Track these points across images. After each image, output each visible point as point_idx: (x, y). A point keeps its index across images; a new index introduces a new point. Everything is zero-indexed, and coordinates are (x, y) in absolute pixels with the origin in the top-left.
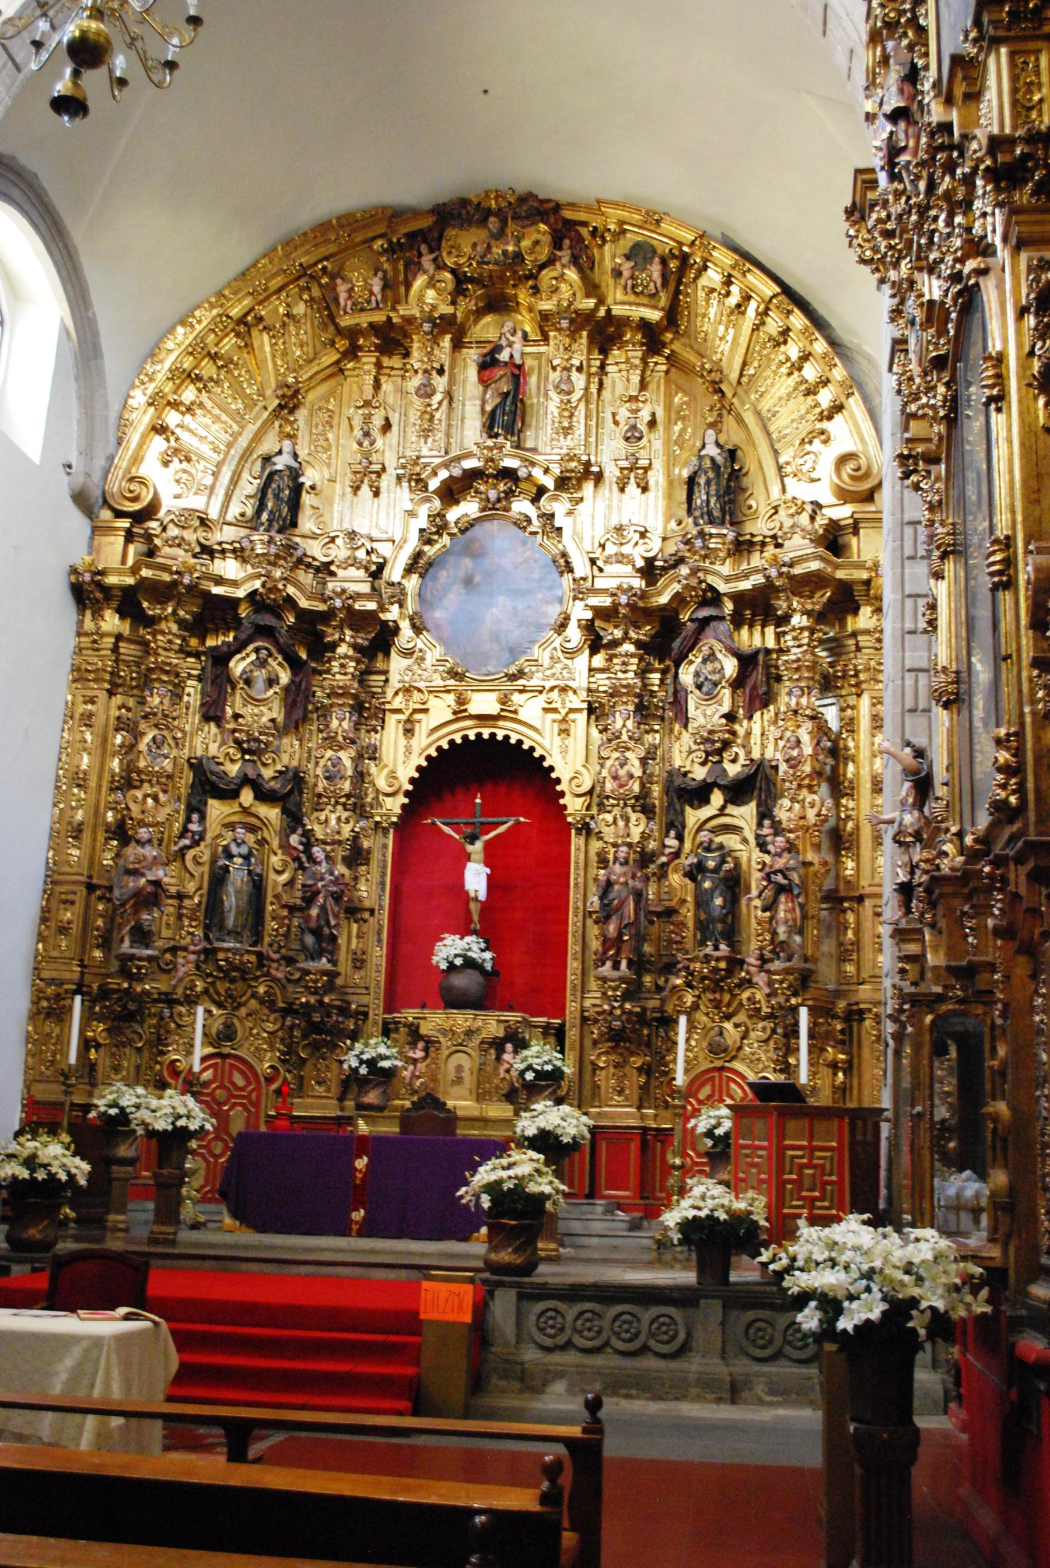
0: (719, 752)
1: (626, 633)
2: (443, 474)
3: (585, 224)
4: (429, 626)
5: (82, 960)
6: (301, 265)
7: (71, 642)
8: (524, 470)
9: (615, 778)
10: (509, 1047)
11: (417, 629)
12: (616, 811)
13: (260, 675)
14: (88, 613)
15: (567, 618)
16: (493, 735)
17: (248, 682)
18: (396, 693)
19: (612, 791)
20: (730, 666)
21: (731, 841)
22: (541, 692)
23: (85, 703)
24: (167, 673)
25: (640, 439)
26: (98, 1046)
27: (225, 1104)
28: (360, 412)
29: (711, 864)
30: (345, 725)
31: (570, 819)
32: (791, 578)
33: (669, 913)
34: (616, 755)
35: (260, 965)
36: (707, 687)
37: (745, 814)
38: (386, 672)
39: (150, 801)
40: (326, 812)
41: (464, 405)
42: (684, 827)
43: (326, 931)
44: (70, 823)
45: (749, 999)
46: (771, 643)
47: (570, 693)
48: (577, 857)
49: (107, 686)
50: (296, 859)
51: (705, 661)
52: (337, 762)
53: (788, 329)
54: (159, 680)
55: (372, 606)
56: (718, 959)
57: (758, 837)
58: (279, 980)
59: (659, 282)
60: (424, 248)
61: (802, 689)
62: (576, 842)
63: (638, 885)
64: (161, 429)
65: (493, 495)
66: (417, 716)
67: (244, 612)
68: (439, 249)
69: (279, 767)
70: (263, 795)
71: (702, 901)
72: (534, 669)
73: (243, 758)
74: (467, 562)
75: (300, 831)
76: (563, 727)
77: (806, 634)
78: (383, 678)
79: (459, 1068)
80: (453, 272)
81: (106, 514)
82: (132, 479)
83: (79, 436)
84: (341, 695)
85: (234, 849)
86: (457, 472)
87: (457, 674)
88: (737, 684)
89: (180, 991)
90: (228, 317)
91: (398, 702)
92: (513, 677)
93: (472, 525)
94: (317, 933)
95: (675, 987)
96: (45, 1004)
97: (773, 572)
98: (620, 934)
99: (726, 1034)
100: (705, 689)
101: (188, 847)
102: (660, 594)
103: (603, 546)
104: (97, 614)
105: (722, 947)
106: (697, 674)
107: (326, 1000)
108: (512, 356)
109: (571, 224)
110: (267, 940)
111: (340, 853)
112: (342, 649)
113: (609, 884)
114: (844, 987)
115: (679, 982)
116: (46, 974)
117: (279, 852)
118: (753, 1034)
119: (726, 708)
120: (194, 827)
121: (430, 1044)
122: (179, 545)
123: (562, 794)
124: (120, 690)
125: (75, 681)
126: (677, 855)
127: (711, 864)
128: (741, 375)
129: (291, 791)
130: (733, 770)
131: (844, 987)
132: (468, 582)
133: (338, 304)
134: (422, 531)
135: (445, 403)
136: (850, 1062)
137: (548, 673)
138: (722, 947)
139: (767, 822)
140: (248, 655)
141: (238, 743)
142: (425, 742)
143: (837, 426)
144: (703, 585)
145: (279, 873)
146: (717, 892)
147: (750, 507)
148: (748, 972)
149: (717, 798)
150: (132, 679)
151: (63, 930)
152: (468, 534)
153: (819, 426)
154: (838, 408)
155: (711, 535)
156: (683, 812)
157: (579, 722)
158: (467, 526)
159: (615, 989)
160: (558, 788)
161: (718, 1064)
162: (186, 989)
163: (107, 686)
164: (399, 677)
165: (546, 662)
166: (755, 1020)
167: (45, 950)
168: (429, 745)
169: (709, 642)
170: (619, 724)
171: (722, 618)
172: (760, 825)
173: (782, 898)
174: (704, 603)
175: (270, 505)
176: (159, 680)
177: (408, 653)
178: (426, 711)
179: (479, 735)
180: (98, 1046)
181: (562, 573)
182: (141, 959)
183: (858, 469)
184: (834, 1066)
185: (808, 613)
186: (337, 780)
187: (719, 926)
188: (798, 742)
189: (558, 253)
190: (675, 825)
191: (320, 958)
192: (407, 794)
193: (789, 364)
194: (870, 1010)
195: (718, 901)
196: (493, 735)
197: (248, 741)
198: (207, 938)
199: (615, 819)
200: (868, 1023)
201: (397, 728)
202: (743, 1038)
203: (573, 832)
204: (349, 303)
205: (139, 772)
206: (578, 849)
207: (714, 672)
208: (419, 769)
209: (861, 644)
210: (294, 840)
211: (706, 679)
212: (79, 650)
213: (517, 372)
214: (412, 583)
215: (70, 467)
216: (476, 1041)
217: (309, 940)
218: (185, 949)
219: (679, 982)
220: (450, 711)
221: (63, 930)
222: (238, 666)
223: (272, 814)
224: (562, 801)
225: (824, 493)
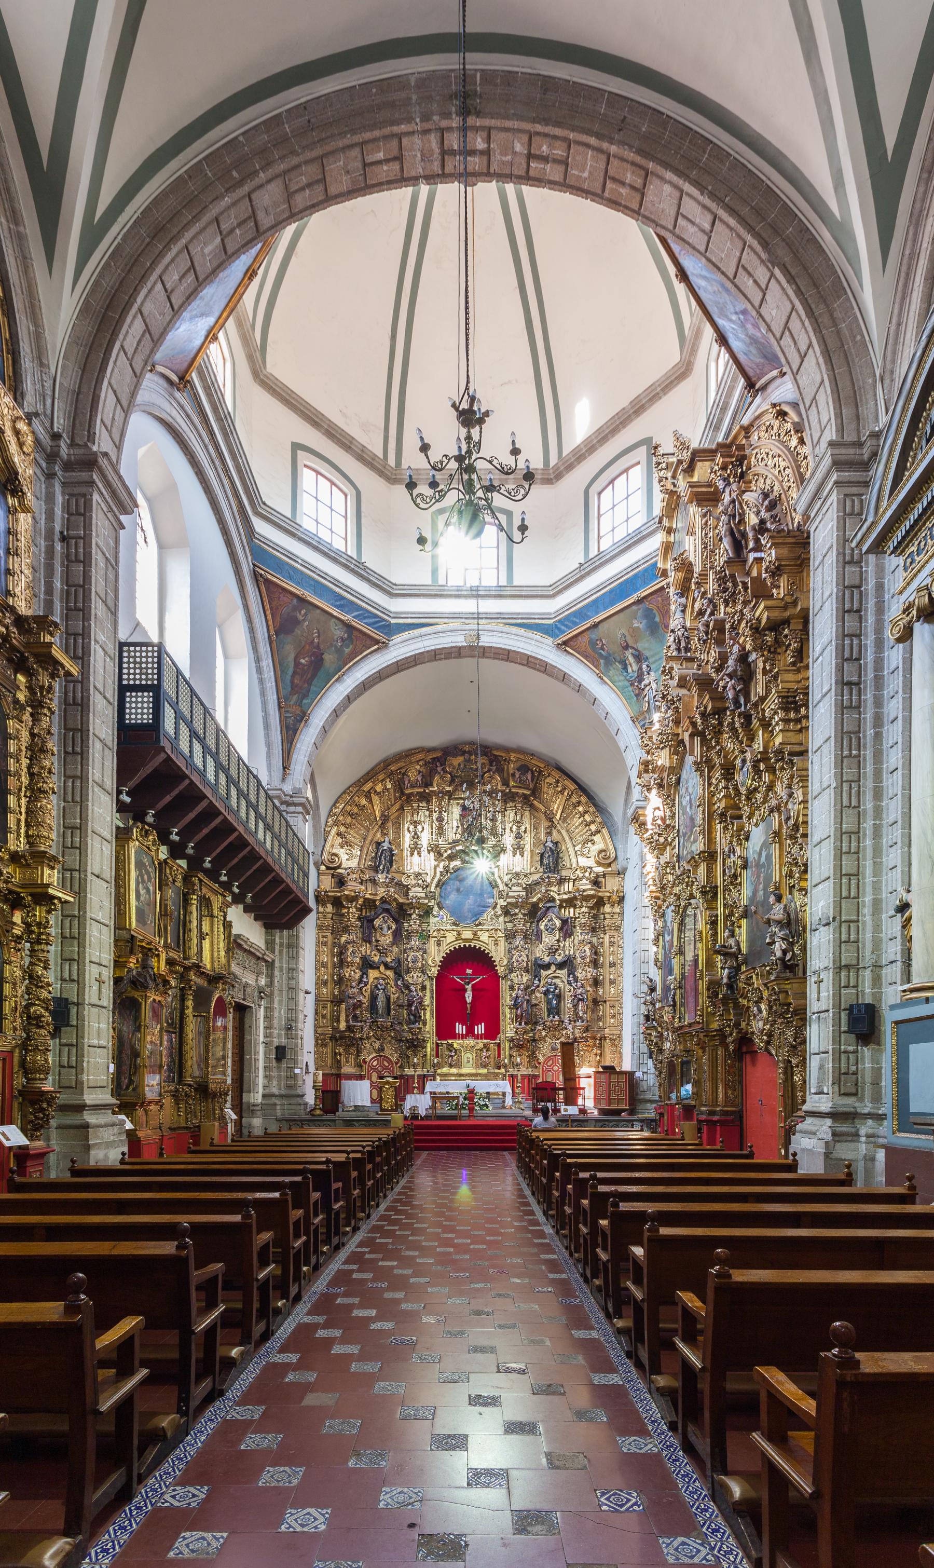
20: (558, 923)
36: (550, 930)
37: (563, 973)
67: (378, 903)
70: (387, 967)
71: (549, 1002)
88: (561, 929)
109: (496, 756)
143: (597, 838)
149: (553, 968)
174: (549, 901)
190: (537, 976)
222: (377, 922)
223: (390, 973)
225: (591, 862)
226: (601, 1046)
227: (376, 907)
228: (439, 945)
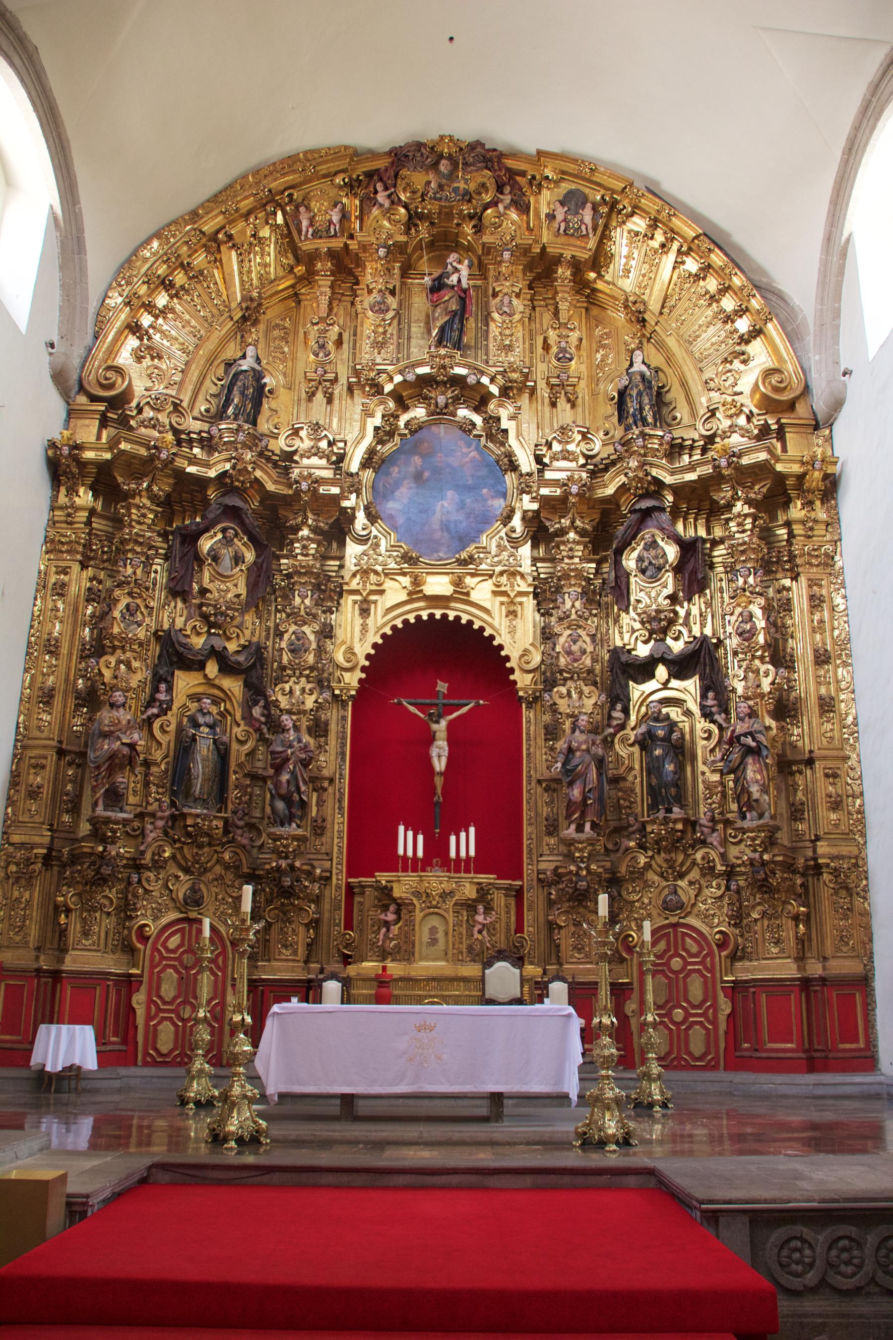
0: (665, 631)
1: (573, 522)
2: (398, 379)
3: (523, 174)
4: (382, 516)
5: (52, 825)
6: (270, 191)
7: (44, 516)
8: (473, 377)
9: (569, 653)
10: (481, 908)
11: (372, 517)
12: (569, 683)
13: (227, 554)
14: (63, 490)
15: (513, 511)
16: (445, 616)
17: (216, 559)
18: (354, 575)
19: (566, 666)
20: (672, 552)
21: (674, 713)
22: (491, 576)
23: (57, 573)
24: (141, 544)
25: (571, 360)
26: (68, 911)
27: (192, 968)
28: (316, 328)
29: (661, 733)
30: (307, 602)
31: (521, 693)
32: (739, 469)
33: (616, 780)
34: (569, 632)
35: (226, 832)
38: (341, 558)
39: (122, 667)
40: (291, 683)
41: (409, 327)
42: (629, 700)
43: (296, 797)
44: (41, 689)
45: (703, 858)
46: (702, 533)
47: (518, 578)
48: (528, 729)
49: (79, 557)
50: (258, 730)
51: (646, 548)
52: (300, 636)
53: (709, 266)
54: (132, 550)
55: (335, 490)
56: (676, 821)
57: (703, 707)
58: (244, 847)
59: (590, 226)
60: (379, 186)
61: (749, 569)
62: (527, 714)
63: (600, 751)
64: (134, 328)
65: (441, 400)
66: (373, 598)
67: (212, 494)
68: (395, 186)
69: (242, 642)
70: (227, 667)
72: (482, 555)
73: (208, 632)
74: (417, 460)
75: (262, 703)
76: (512, 608)
77: (749, 520)
78: (338, 563)
79: (433, 930)
80: (406, 207)
81: (82, 399)
82: (109, 368)
83: (61, 322)
84: (305, 574)
85: (201, 720)
86: (411, 377)
87: (411, 558)
89: (148, 856)
90: (201, 231)
91: (355, 584)
92: (463, 563)
93: (421, 428)
94: (287, 799)
95: (628, 849)
96: (13, 868)
97: (723, 462)
98: (585, 798)
99: (680, 892)
100: (648, 573)
101: (157, 716)
102: (605, 486)
103: (549, 445)
104: (72, 491)
105: (676, 809)
106: (640, 559)
107: (297, 864)
108: (459, 281)
110: (230, 807)
111: (304, 723)
112: (305, 532)
113: (570, 751)
114: (799, 844)
115: (632, 844)
116: (15, 839)
117: (242, 723)
118: (707, 892)
119: (670, 590)
120: (162, 696)
121: (400, 906)
122: (154, 427)
123: (512, 671)
124: (92, 563)
125: (47, 552)
126: (622, 727)
127: (661, 733)
128: (663, 307)
129: (253, 666)
130: (677, 647)
131: (799, 844)
132: (418, 477)
133: (300, 232)
134: (377, 429)
135: (395, 322)
136: (808, 915)
137: (496, 559)
138: (676, 809)
139: (711, 694)
140: (215, 534)
141: (205, 617)
142: (380, 621)
143: (756, 348)
144: (649, 478)
145: (242, 743)
146: (668, 759)
147: (675, 418)
148: (702, 833)
149: (661, 672)
150: (103, 552)
151: (33, 794)
152: (417, 435)
153: (737, 348)
154: (756, 333)
155: (651, 436)
156: (627, 685)
157: (525, 605)
158: (415, 428)
159: (581, 850)
160: (508, 665)
161: (673, 920)
162: (154, 854)
163: (79, 557)
164: (354, 561)
165: (494, 550)
166: (708, 878)
167: (14, 814)
168: (385, 625)
169: (649, 532)
170: (568, 604)
171: (663, 510)
172: (704, 696)
173: (750, 760)
175: (236, 401)
176: (132, 550)
177: (362, 540)
178: (382, 592)
179: (432, 616)
180: (68, 911)
181: (506, 470)
182: (116, 822)
183: (781, 382)
184: (796, 918)
185: (748, 502)
186: (302, 652)
187: (673, 791)
188: (751, 616)
189: (501, 197)
191: (290, 824)
192: (364, 669)
193: (708, 296)
194: (828, 865)
195: (670, 767)
196: (445, 616)
197: (215, 615)
198: (173, 804)
199: (569, 692)
200: (826, 877)
201: (353, 608)
202: (696, 896)
203: (524, 706)
204: (311, 231)
205: (112, 637)
206: (529, 722)
207: (656, 557)
208: (375, 646)
209: (796, 532)
210: (257, 711)
211: (650, 563)
212: (52, 523)
213: (463, 295)
214: (368, 475)
215: (52, 346)
216: (450, 903)
217: (280, 805)
218: (153, 815)
219: (632, 844)
220: (406, 591)
221: (33, 794)
222: (206, 544)
223: (234, 686)
224: (512, 677)
226: (805, 895)
227: (206, 502)
228: (365, 612)
